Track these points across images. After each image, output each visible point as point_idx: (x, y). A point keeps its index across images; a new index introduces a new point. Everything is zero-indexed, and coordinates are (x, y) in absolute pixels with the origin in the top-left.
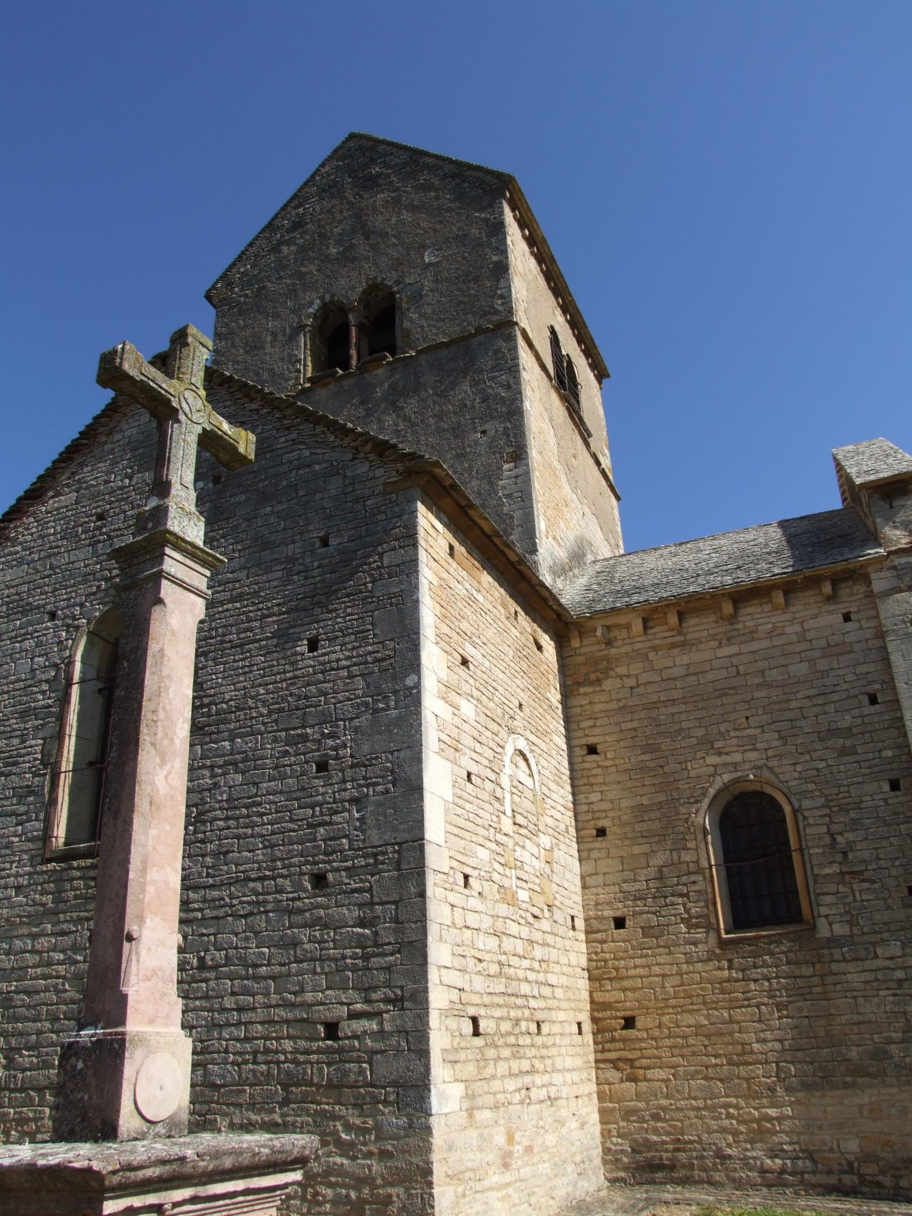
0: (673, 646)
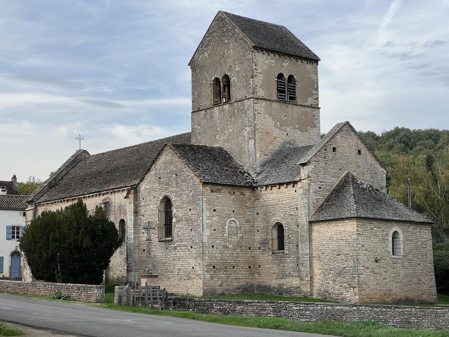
0: (271, 193)
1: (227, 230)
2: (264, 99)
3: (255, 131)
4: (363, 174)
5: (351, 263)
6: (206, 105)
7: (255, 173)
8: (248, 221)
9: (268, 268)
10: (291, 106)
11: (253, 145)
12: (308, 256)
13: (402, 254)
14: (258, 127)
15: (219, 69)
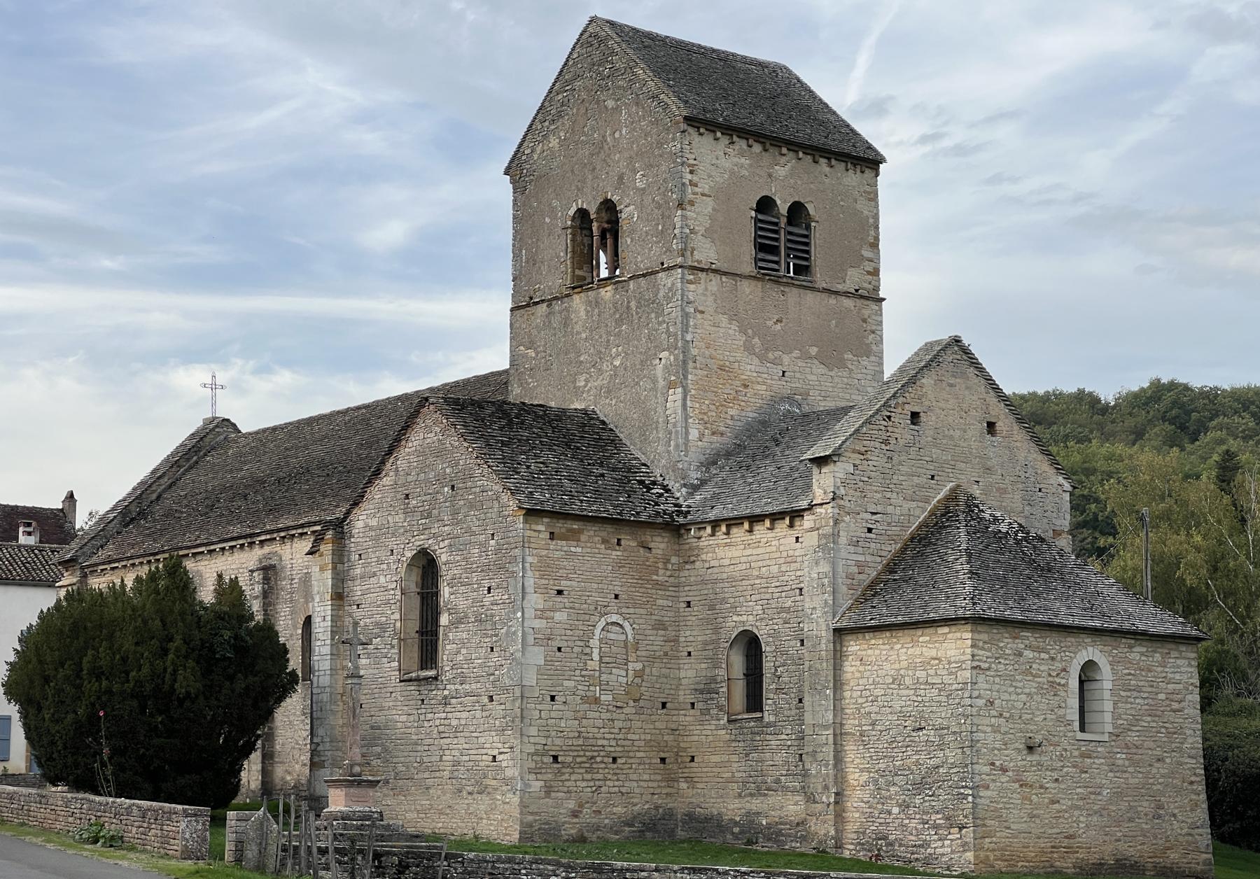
0: (726, 545)
1: (596, 651)
2: (716, 271)
3: (684, 362)
4: (1003, 491)
5: (952, 755)
6: (550, 288)
7: (685, 485)
8: (660, 626)
9: (716, 765)
10: (795, 290)
11: (679, 403)
12: (831, 731)
13: (1109, 728)
14: (694, 352)
15: (589, 183)
